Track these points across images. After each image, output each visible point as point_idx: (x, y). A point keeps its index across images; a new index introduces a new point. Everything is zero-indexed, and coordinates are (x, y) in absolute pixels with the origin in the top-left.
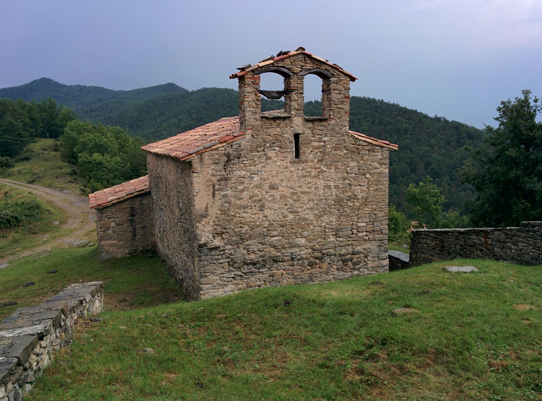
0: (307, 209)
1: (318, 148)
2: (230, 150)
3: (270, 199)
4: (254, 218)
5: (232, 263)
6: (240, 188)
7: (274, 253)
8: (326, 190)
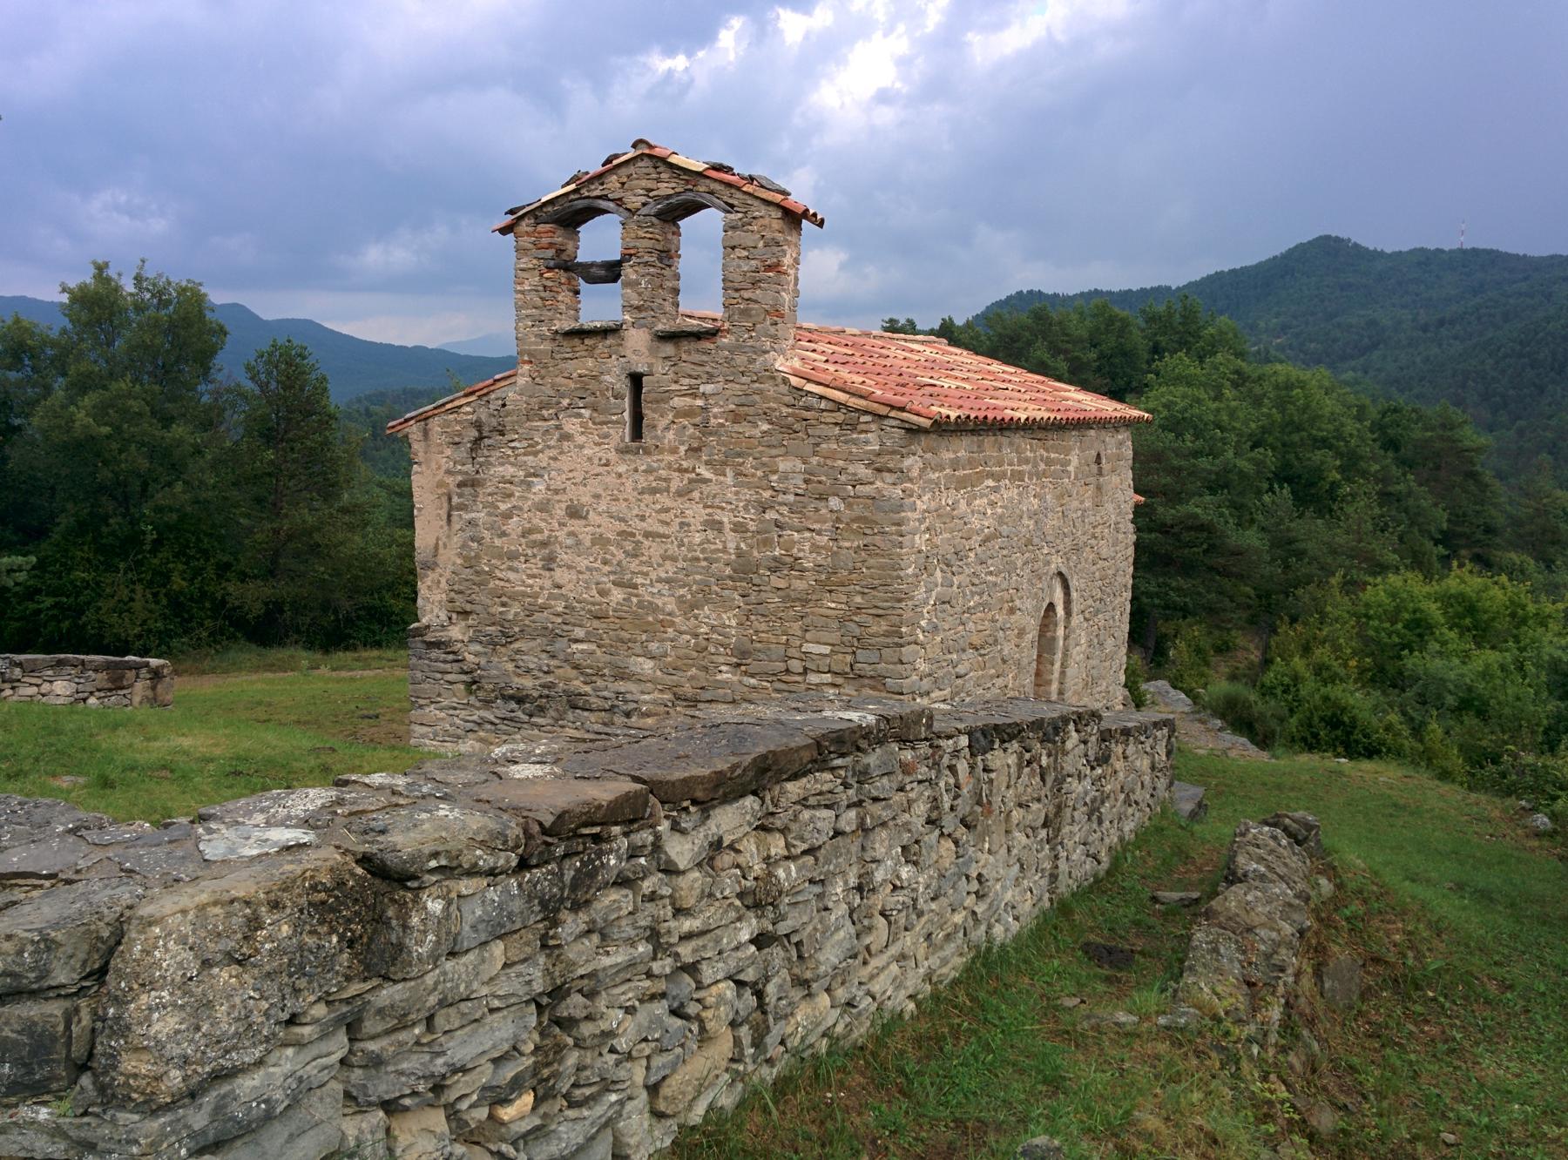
0: (660, 580)
1: (688, 413)
2: (483, 414)
3: (569, 542)
4: (531, 586)
5: (473, 685)
6: (503, 507)
7: (578, 684)
8: (710, 534)
